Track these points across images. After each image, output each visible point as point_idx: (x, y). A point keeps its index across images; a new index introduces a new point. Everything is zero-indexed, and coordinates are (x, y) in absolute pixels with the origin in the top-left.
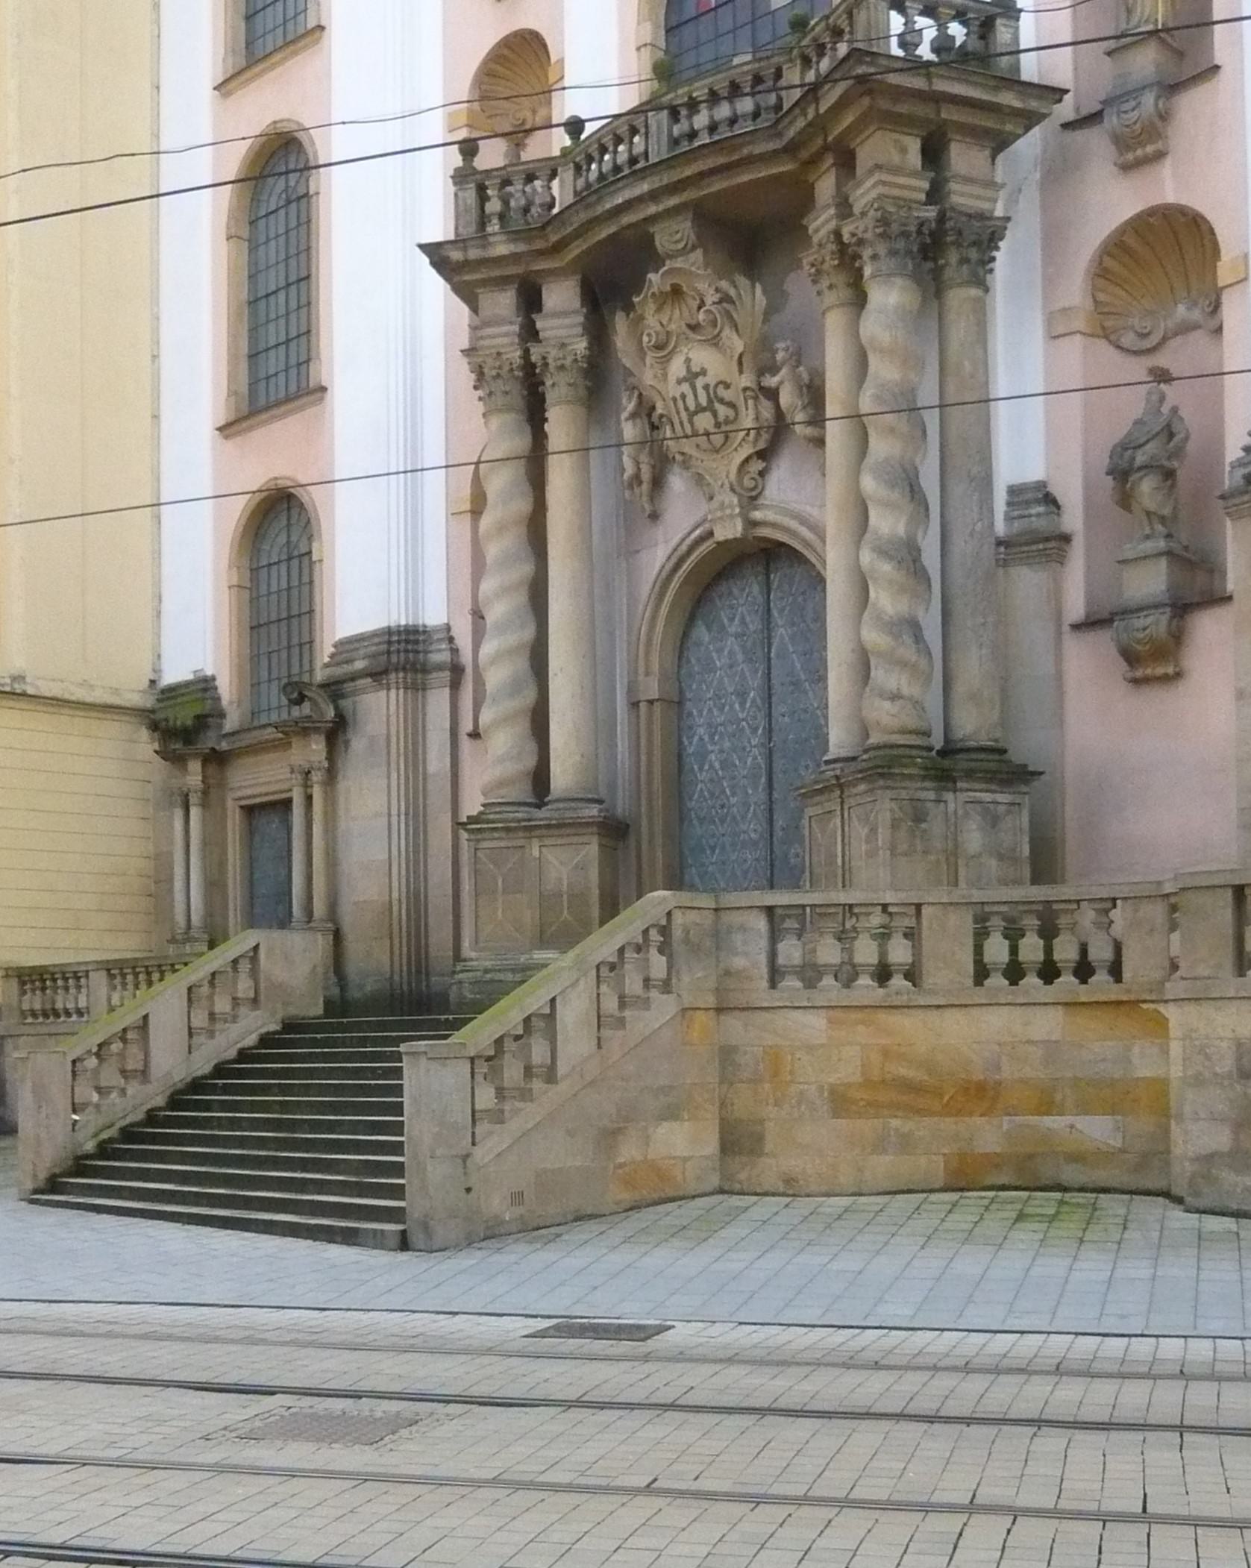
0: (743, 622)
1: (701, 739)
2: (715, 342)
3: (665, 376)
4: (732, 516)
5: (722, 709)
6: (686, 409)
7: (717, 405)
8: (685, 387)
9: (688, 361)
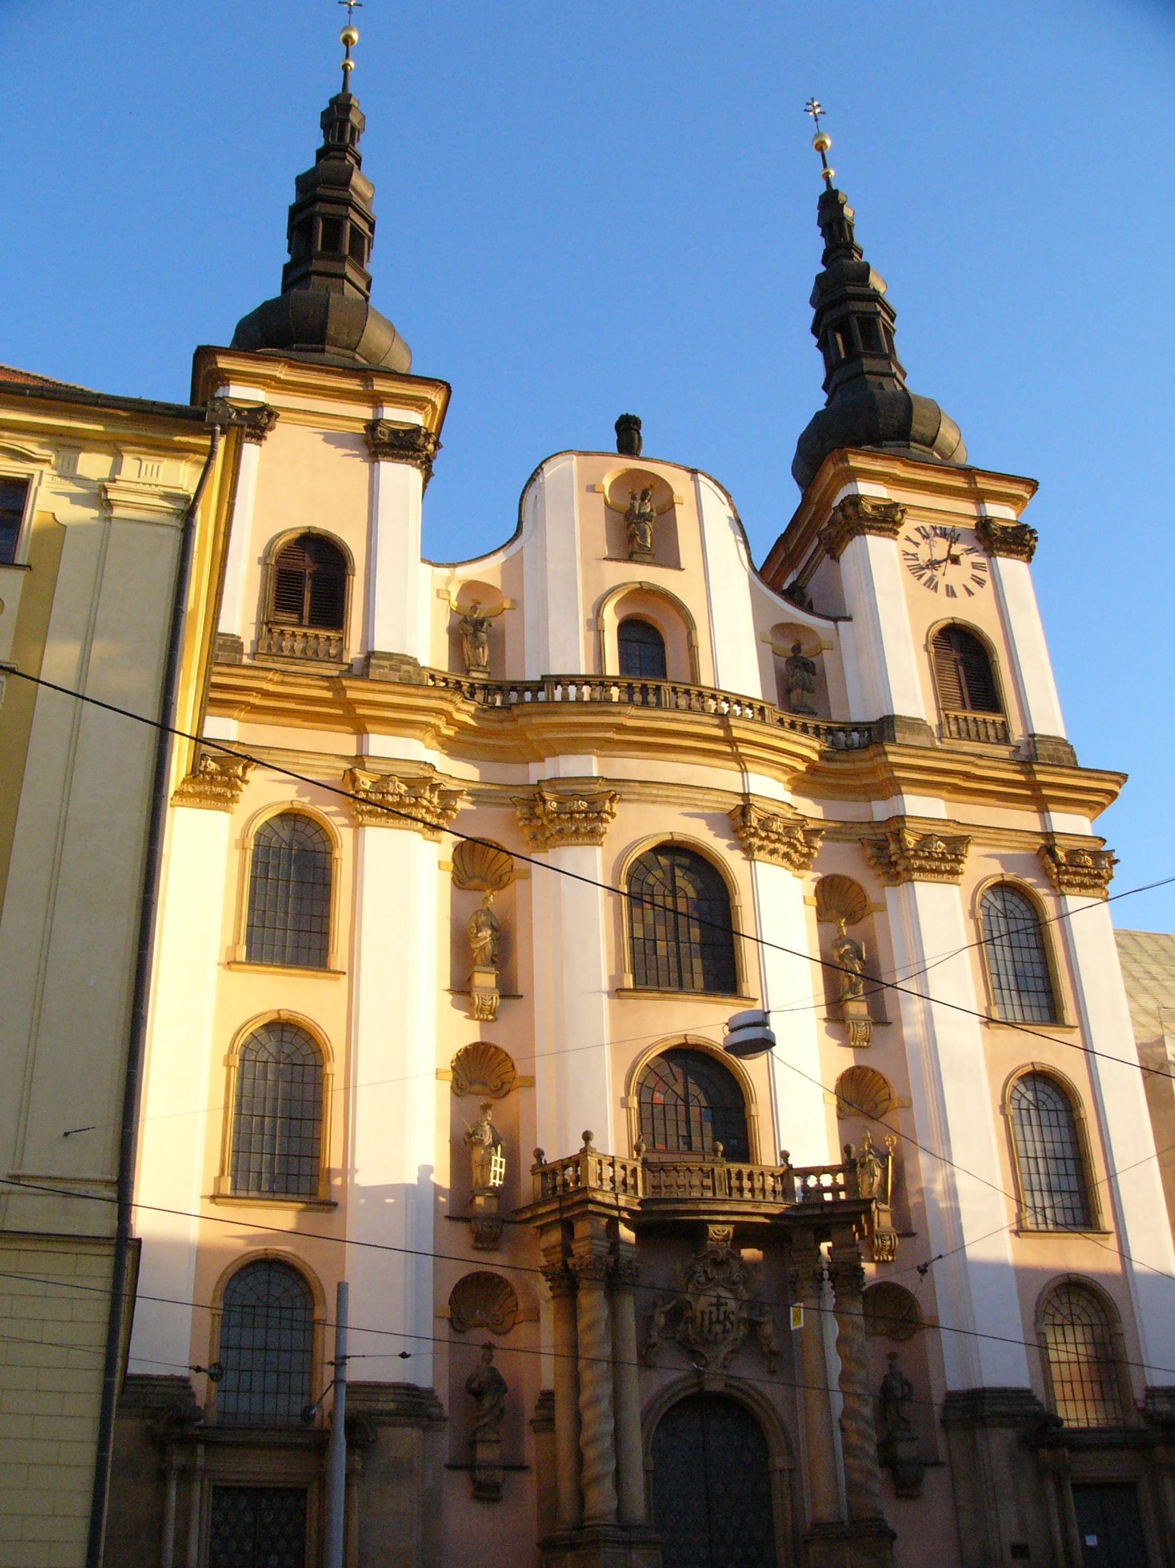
6: (710, 1319)
8: (714, 1309)
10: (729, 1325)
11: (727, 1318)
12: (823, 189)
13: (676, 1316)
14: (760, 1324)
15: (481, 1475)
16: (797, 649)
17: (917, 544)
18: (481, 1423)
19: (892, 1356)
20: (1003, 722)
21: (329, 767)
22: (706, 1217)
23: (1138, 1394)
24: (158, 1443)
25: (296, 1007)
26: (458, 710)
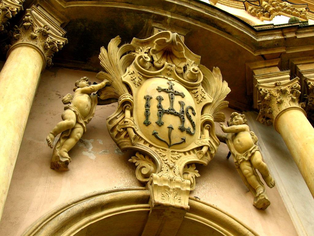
3: (139, 85)
6: (160, 107)
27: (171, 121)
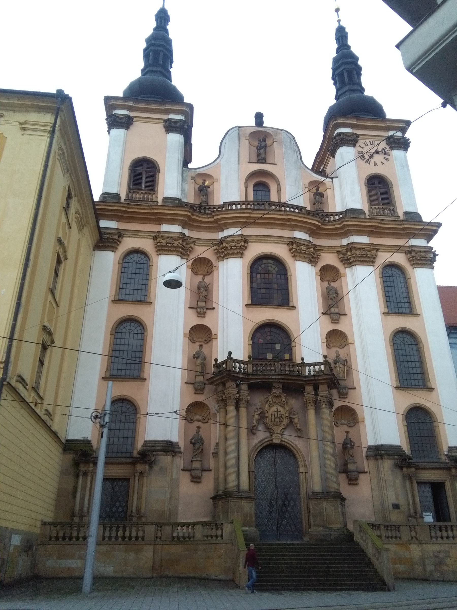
0: (269, 458)
1: (259, 481)
2: (282, 407)
4: (278, 439)
5: (264, 476)
6: (274, 417)
7: (281, 418)
8: (276, 413)
9: (277, 408)
10: (281, 419)
11: (281, 416)
12: (337, 25)
13: (262, 416)
14: (294, 419)
15: (194, 473)
16: (317, 189)
17: (363, 148)
18: (195, 454)
19: (347, 432)
20: (394, 209)
21: (148, 236)
22: (272, 381)
23: (445, 450)
24: (76, 464)
25: (135, 314)
26: (192, 214)
27: (277, 420)
